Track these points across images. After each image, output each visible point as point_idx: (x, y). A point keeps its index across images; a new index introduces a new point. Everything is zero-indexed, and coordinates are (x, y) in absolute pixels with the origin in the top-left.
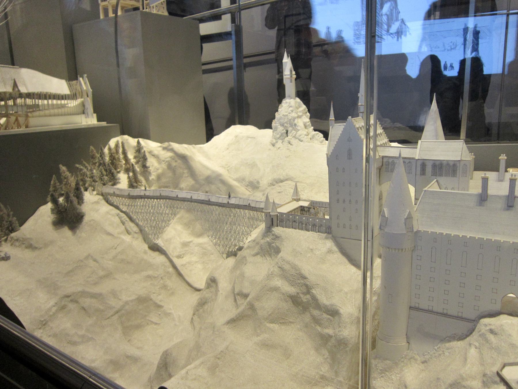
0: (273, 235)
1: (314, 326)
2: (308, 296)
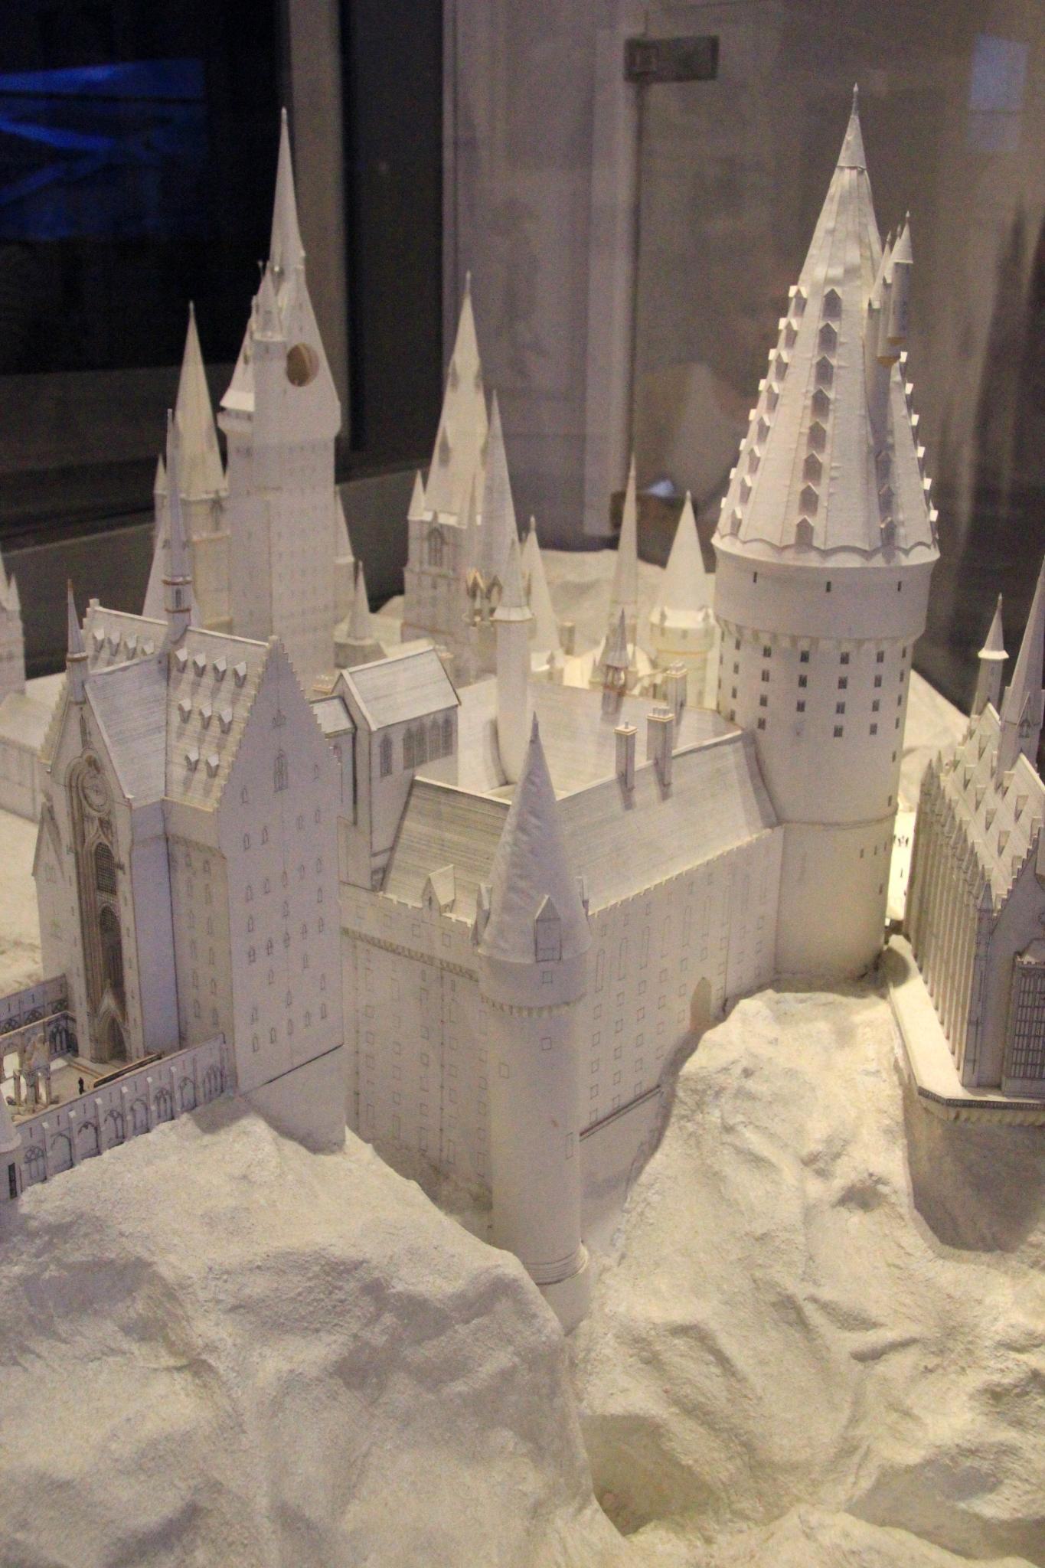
0: (32, 1235)
1: (431, 1397)
2: (388, 1319)
